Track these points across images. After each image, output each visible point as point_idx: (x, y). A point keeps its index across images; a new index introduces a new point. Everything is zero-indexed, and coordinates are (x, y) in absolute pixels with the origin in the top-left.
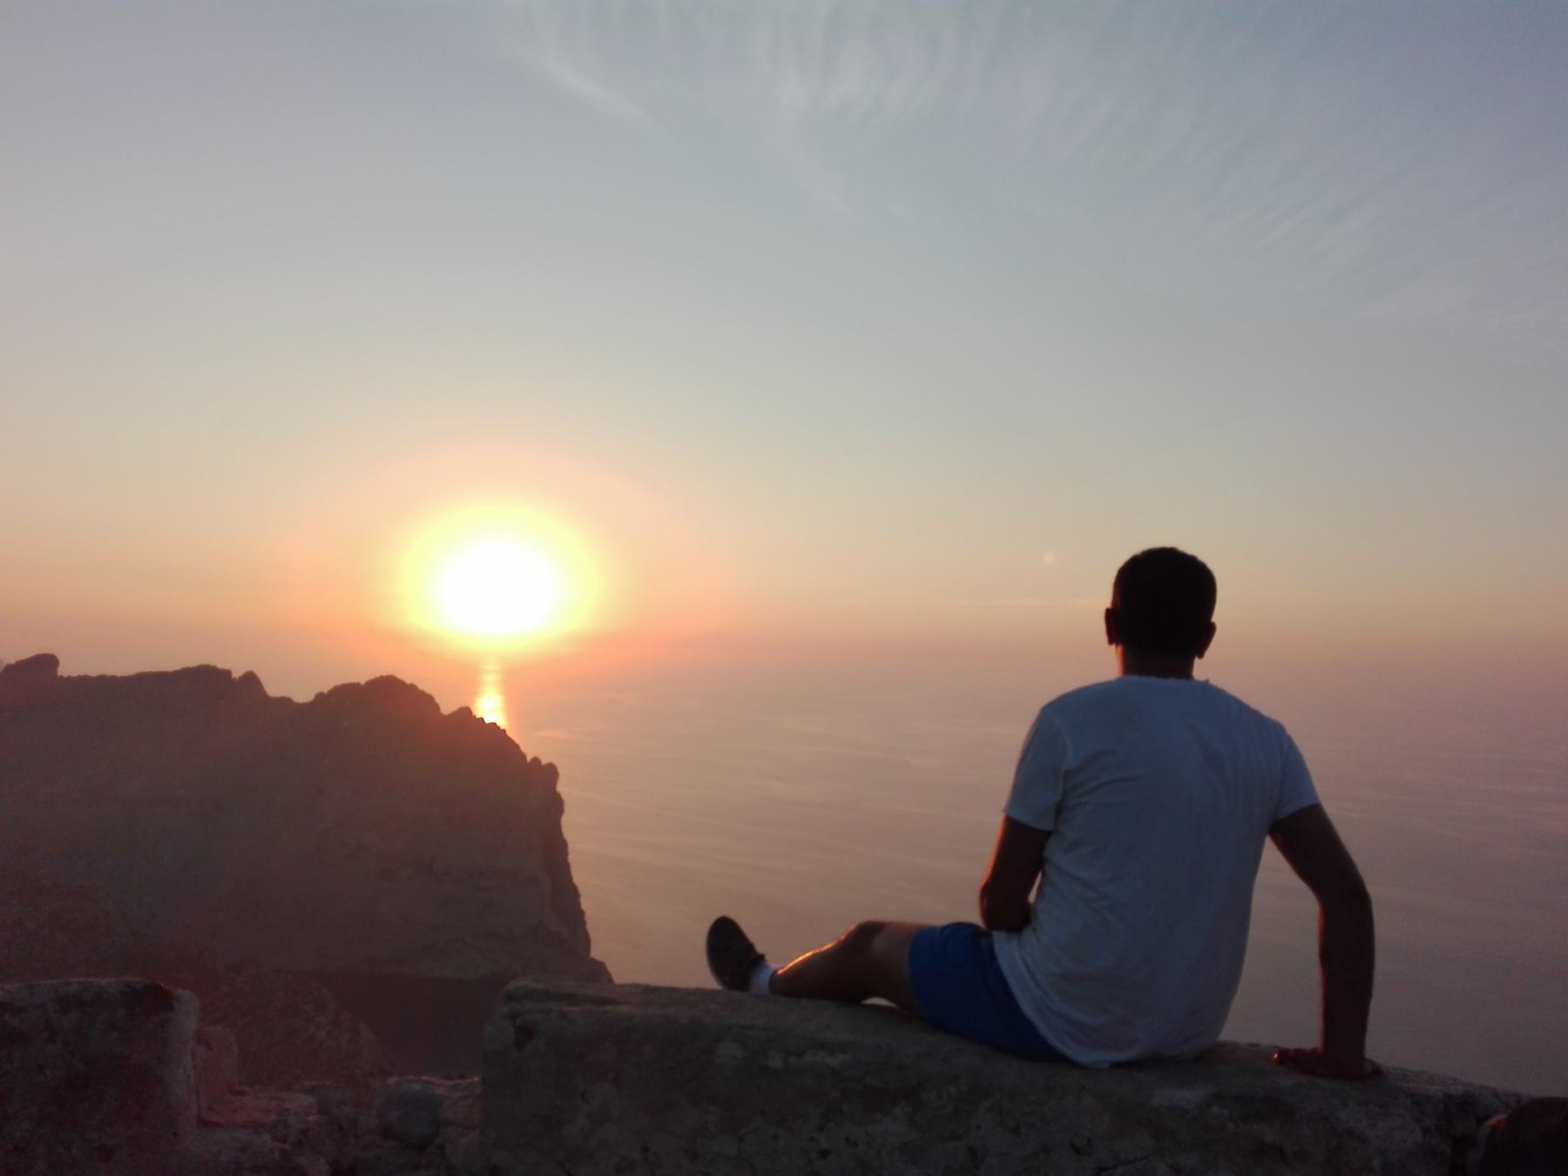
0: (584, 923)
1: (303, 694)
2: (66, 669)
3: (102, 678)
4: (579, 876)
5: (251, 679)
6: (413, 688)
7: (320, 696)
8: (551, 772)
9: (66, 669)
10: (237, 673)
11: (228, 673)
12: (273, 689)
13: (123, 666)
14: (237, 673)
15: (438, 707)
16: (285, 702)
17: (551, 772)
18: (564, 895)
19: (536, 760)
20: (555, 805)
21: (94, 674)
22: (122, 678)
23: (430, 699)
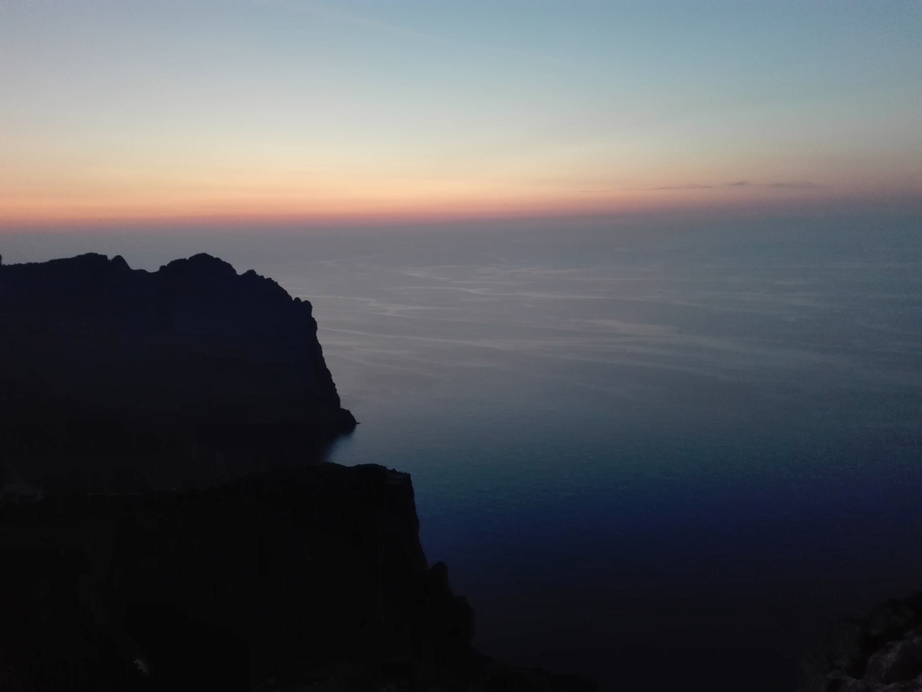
1: (153, 267)
3: (30, 264)
4: (329, 365)
5: (119, 260)
6: (218, 260)
7: (162, 268)
8: (307, 306)
11: (105, 257)
12: (134, 265)
13: (42, 256)
15: (234, 271)
16: (142, 272)
17: (307, 306)
19: (297, 299)
20: (312, 325)
21: (24, 262)
22: (41, 264)
23: (229, 266)
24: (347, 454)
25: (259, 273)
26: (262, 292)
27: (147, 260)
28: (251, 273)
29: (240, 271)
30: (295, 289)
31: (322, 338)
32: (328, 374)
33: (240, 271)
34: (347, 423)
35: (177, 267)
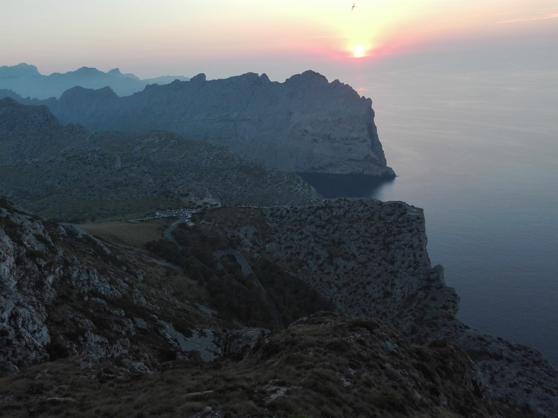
0: (384, 155)
1: (282, 80)
2: (208, 79)
3: (219, 80)
5: (264, 75)
6: (318, 74)
8: (369, 101)
9: (208, 79)
10: (260, 75)
13: (225, 76)
14: (260, 75)
15: (327, 81)
16: (276, 83)
18: (376, 146)
19: (363, 97)
23: (324, 77)
24: (388, 194)
25: (341, 81)
26: (343, 92)
27: (279, 76)
28: (337, 81)
29: (330, 81)
30: (361, 91)
31: (377, 121)
32: (380, 145)
33: (330, 81)
34: (389, 176)
35: (295, 80)
